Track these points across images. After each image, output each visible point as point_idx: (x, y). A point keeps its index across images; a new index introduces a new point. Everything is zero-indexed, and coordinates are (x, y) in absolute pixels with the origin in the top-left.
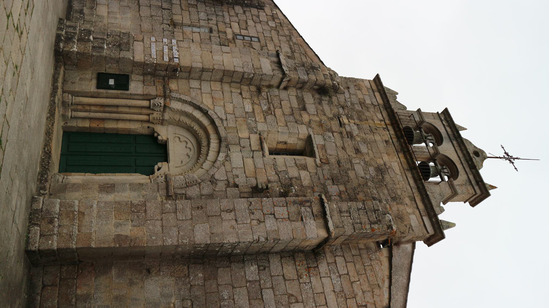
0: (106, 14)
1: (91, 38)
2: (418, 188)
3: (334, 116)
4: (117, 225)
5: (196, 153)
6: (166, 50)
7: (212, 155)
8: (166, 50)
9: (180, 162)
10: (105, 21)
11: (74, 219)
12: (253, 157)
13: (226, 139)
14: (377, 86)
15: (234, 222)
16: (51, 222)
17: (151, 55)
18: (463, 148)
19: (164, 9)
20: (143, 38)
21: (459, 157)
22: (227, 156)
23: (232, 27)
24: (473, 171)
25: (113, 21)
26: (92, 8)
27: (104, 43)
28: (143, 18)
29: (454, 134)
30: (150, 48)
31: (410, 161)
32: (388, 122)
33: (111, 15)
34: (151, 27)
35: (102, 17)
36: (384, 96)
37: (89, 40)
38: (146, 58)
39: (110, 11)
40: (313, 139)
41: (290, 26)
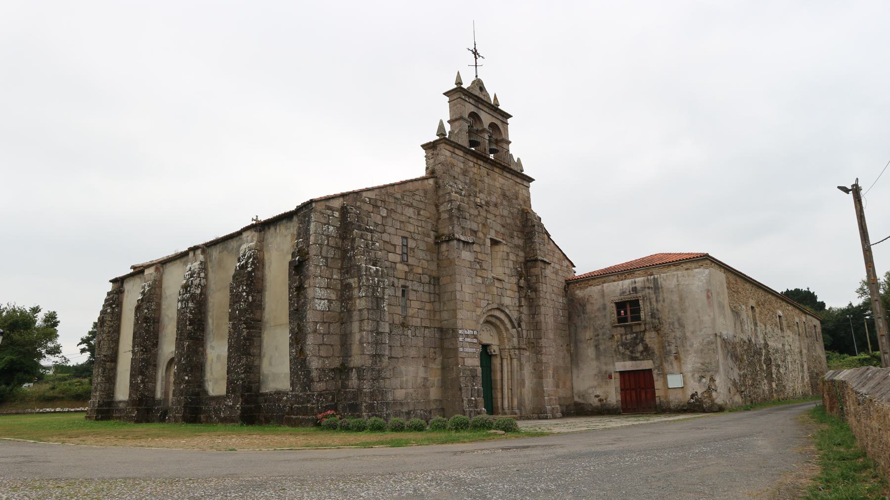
0: (404, 391)
1: (473, 398)
2: (512, 174)
3: (477, 209)
4: (550, 378)
5: (488, 325)
6: (469, 340)
7: (502, 316)
8: (469, 340)
9: (491, 337)
10: (411, 391)
11: (551, 399)
12: (506, 289)
13: (498, 305)
14: (451, 145)
15: (548, 317)
16: (553, 408)
17: (474, 353)
18: (485, 103)
19: (391, 332)
20: (461, 357)
21: (489, 114)
22: (507, 307)
23: (394, 261)
24: (498, 111)
25: (410, 384)
26: (401, 404)
27: (475, 389)
28: (405, 355)
29: (475, 100)
30: (468, 352)
31: (501, 167)
32: (475, 160)
33: (405, 386)
34: (413, 348)
35: (407, 394)
36: (460, 147)
37: (476, 400)
38: (476, 356)
39: (399, 387)
40: (492, 237)
41: (383, 191)
